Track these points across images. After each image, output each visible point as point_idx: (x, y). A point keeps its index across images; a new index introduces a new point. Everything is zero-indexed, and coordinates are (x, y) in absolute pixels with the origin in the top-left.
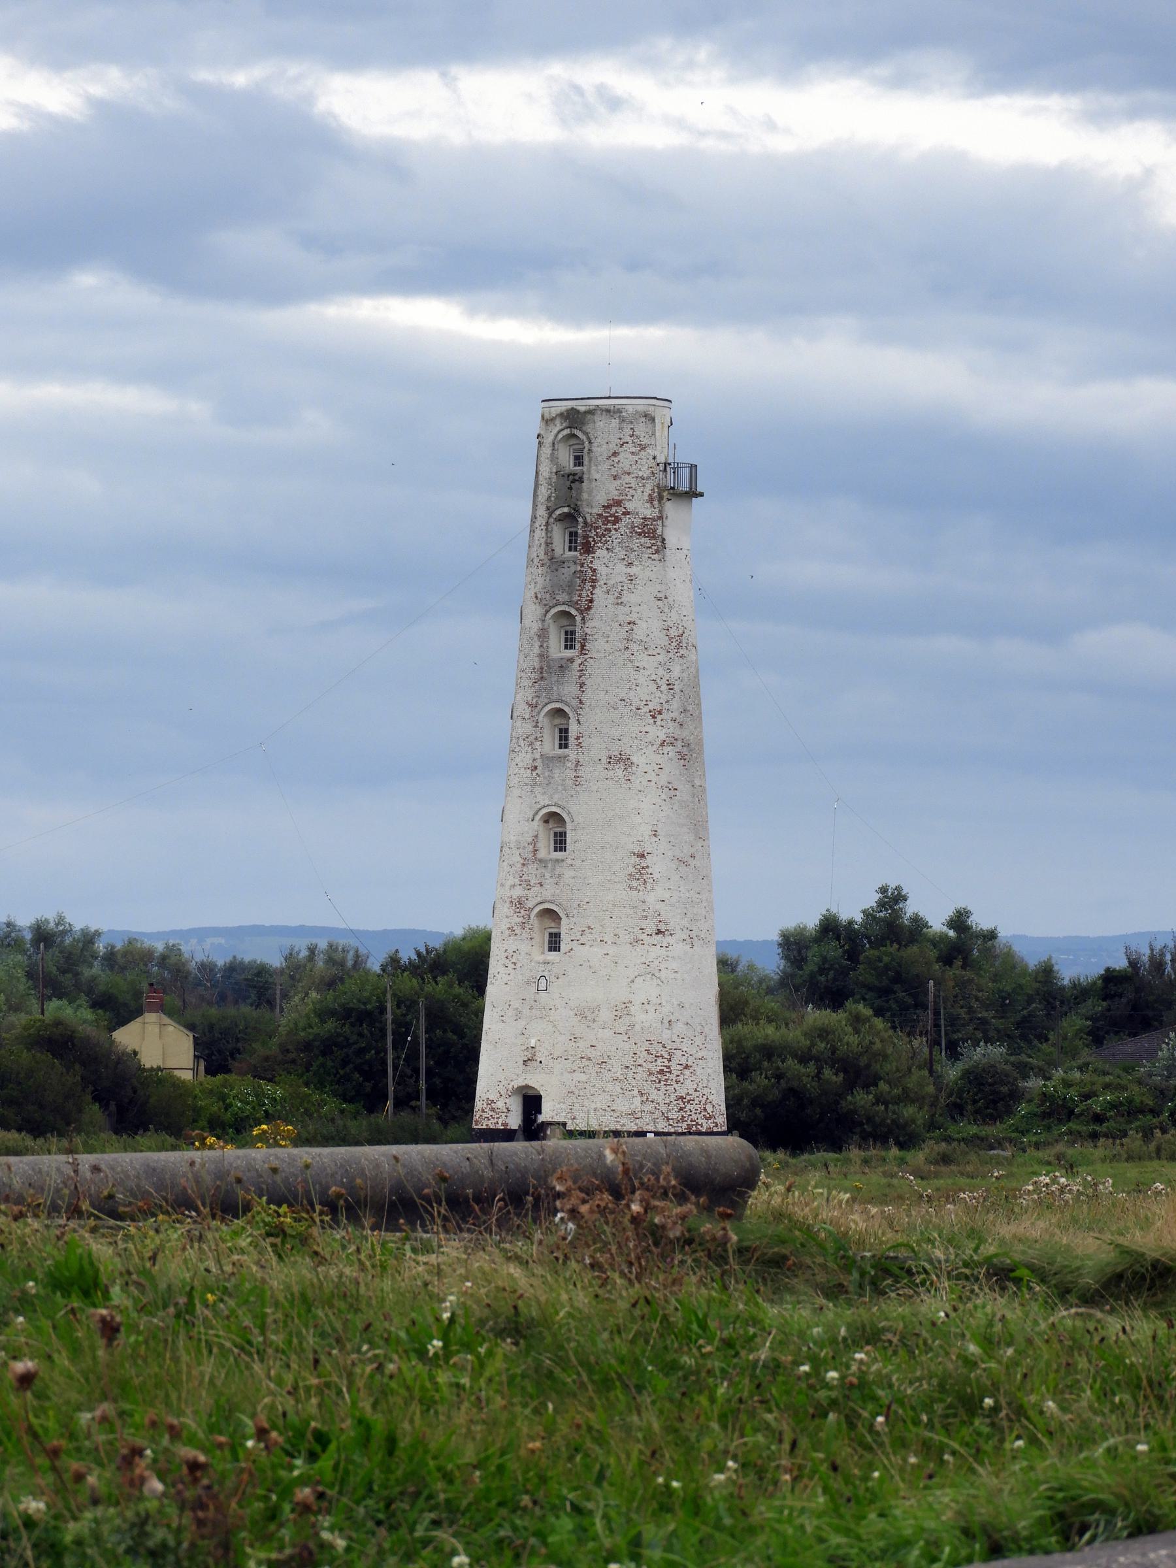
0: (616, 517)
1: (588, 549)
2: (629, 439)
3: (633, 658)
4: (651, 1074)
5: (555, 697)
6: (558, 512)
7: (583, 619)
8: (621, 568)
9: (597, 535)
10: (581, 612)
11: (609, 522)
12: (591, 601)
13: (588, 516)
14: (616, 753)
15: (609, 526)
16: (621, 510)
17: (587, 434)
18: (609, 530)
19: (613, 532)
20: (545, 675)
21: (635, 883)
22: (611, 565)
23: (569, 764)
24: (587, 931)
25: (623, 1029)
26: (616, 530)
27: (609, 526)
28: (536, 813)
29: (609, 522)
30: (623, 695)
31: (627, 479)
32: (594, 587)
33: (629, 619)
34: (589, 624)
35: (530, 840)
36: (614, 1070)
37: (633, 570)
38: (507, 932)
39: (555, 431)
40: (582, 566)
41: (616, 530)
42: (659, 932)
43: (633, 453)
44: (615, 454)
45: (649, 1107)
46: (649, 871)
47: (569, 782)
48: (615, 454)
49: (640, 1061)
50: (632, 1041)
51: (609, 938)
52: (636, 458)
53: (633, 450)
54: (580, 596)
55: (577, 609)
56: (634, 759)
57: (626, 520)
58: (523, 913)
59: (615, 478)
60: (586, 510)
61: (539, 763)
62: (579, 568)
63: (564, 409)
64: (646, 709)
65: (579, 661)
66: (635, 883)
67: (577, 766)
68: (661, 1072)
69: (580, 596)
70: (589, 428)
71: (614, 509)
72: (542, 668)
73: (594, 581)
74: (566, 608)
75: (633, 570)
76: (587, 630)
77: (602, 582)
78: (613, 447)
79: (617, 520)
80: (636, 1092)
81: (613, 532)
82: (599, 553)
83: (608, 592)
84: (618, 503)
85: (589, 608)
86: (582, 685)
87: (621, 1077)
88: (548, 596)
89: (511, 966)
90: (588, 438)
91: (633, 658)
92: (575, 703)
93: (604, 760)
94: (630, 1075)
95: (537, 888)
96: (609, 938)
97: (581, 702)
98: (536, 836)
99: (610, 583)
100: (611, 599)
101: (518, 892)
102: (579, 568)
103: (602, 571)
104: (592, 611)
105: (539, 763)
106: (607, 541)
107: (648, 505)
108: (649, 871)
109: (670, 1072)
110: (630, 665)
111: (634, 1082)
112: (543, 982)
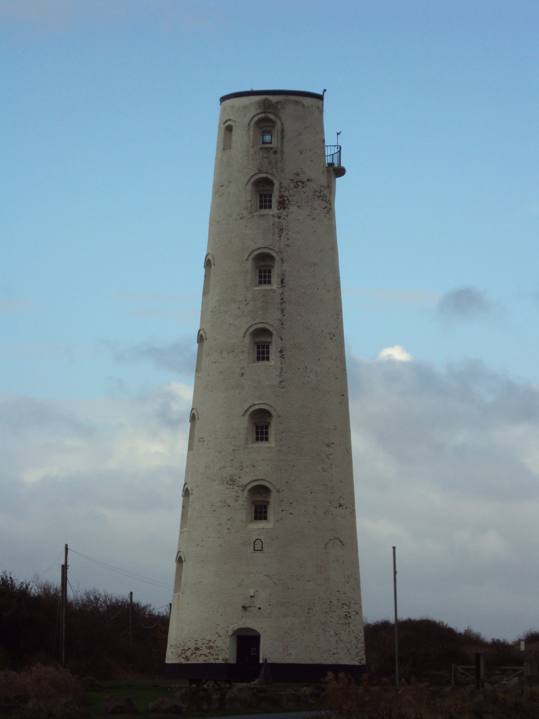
17: (279, 118)
86: (283, 310)
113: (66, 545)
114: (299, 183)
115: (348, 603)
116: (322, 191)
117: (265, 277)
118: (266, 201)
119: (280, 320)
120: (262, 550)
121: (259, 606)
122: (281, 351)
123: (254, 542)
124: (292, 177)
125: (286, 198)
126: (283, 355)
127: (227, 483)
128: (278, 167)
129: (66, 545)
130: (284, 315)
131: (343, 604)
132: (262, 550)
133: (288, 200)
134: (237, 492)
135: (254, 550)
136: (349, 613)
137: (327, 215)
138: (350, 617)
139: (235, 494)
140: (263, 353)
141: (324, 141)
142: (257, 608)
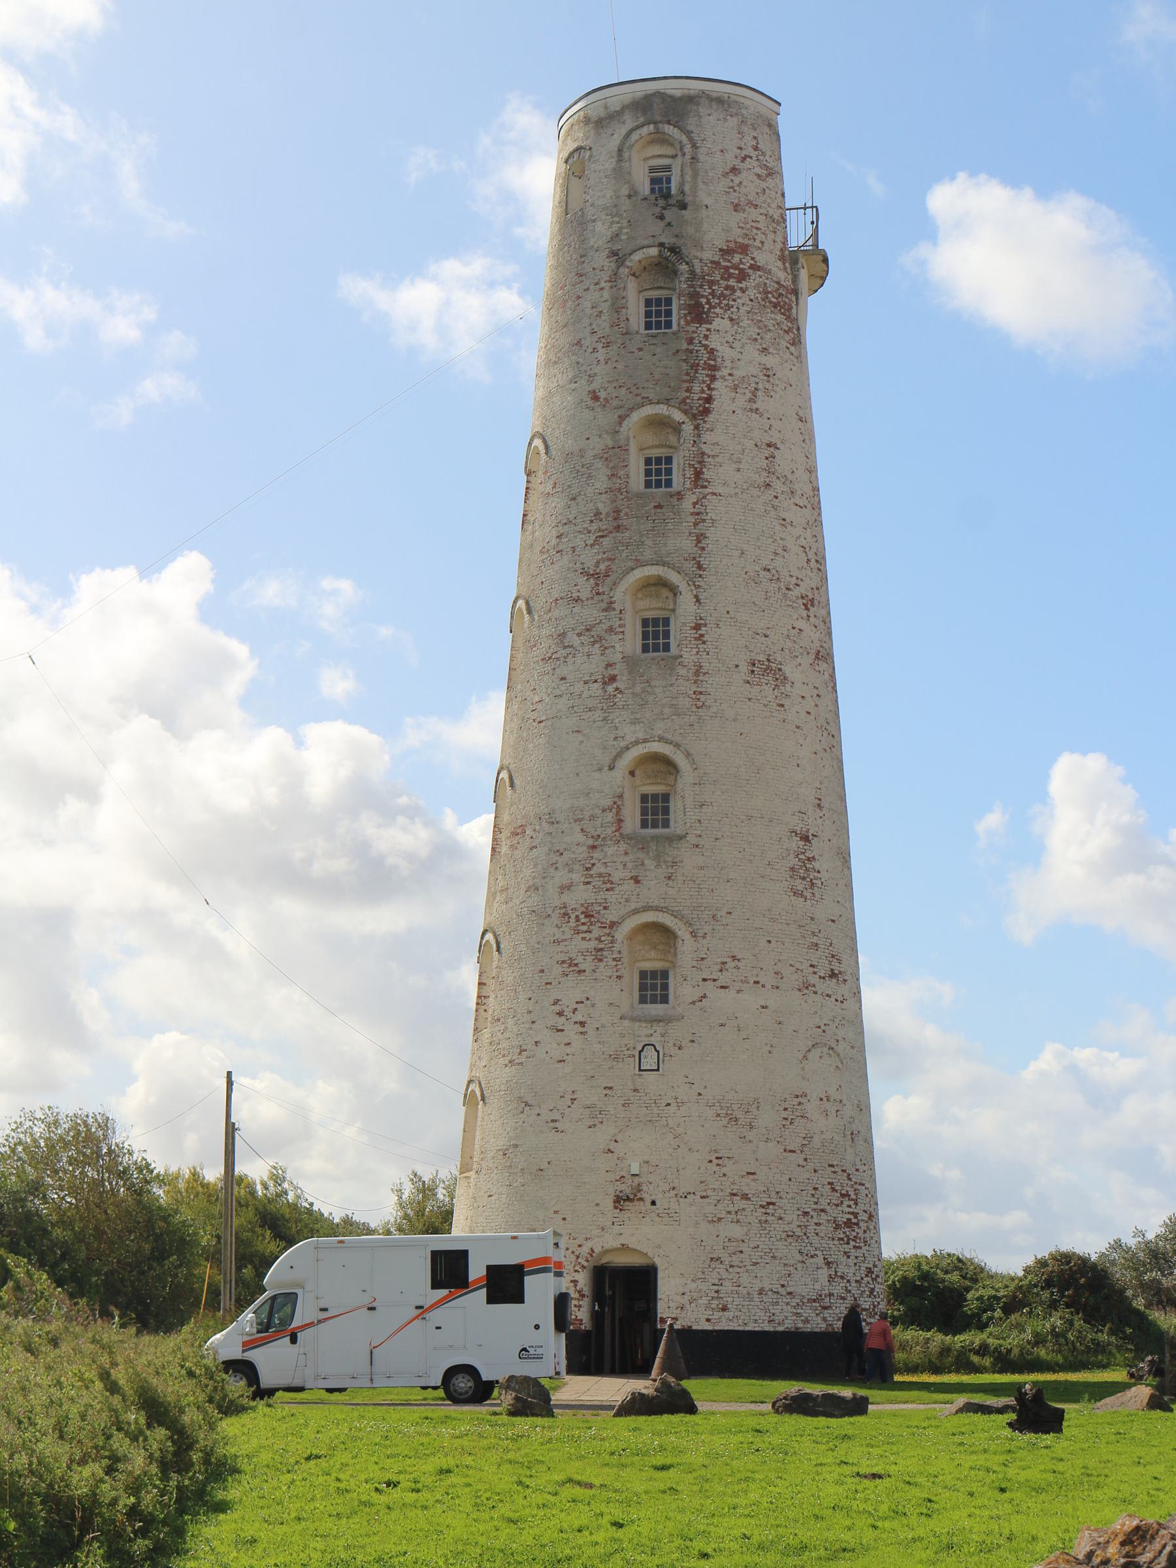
0: (742, 271)
1: (698, 314)
2: (753, 154)
3: (776, 502)
4: (837, 1227)
5: (648, 554)
6: (637, 257)
7: (697, 427)
8: (751, 352)
9: (713, 294)
10: (694, 417)
11: (731, 276)
12: (709, 400)
13: (696, 262)
14: (762, 657)
15: (732, 282)
16: (748, 262)
17: (688, 134)
18: (733, 290)
19: (738, 293)
20: (624, 522)
21: (800, 885)
22: (737, 344)
23: (683, 672)
24: (731, 964)
25: (795, 1144)
26: (743, 291)
27: (732, 282)
28: (619, 755)
29: (731, 276)
30: (765, 562)
31: (754, 214)
32: (713, 378)
33: (767, 439)
34: (706, 437)
35: (608, 802)
36: (788, 1218)
37: (769, 361)
38: (557, 970)
39: (624, 131)
40: (690, 341)
41: (743, 291)
42: (833, 975)
43: (758, 176)
44: (734, 170)
45: (838, 1288)
46: (817, 865)
47: (685, 702)
48: (734, 170)
49: (823, 1203)
50: (810, 1166)
51: (768, 979)
52: (764, 185)
53: (758, 170)
54: (688, 390)
55: (685, 412)
56: (787, 670)
57: (755, 279)
58: (596, 932)
59: (737, 208)
60: (691, 252)
61: (619, 670)
62: (685, 346)
63: (639, 95)
64: (797, 592)
65: (694, 498)
66: (800, 885)
67: (697, 673)
68: (848, 1223)
69: (688, 390)
70: (691, 123)
71: (737, 258)
72: (617, 512)
73: (714, 368)
74: (662, 409)
75: (769, 361)
76: (706, 449)
77: (725, 372)
78: (730, 159)
79: (742, 276)
80: (820, 1260)
81: (738, 293)
82: (717, 323)
83: (735, 388)
84: (744, 249)
85: (706, 412)
86: (700, 538)
87: (798, 1232)
88: (623, 391)
89: (571, 1031)
90: (691, 139)
91: (776, 502)
92: (690, 566)
93: (744, 668)
94: (812, 1228)
95: (629, 886)
96: (768, 979)
97: (700, 567)
98: (621, 796)
99: (738, 374)
100: (741, 401)
101: (580, 896)
102: (685, 346)
103: (724, 351)
104: (711, 418)
105: (619, 670)
106: (729, 307)
107: (779, 264)
108: (817, 865)
109: (857, 1224)
110: (773, 513)
111: (815, 1241)
112: (649, 1060)
113: (229, 1074)
114: (732, 271)
115: (852, 1193)
116: (780, 295)
117: (659, 472)
118: (658, 314)
119: (694, 559)
120: (658, 1070)
121: (653, 1198)
122: (697, 627)
123: (640, 1052)
124: (716, 259)
125: (704, 301)
126: (702, 636)
127: (577, 919)
128: (682, 263)
129: (229, 1074)
130: (703, 549)
131: (843, 1195)
132: (658, 1070)
133: (708, 302)
134: (599, 939)
135: (640, 1070)
136: (855, 1215)
137: (792, 349)
138: (857, 1224)
139: (593, 944)
140: (656, 635)
141: (783, 195)
142: (648, 1203)
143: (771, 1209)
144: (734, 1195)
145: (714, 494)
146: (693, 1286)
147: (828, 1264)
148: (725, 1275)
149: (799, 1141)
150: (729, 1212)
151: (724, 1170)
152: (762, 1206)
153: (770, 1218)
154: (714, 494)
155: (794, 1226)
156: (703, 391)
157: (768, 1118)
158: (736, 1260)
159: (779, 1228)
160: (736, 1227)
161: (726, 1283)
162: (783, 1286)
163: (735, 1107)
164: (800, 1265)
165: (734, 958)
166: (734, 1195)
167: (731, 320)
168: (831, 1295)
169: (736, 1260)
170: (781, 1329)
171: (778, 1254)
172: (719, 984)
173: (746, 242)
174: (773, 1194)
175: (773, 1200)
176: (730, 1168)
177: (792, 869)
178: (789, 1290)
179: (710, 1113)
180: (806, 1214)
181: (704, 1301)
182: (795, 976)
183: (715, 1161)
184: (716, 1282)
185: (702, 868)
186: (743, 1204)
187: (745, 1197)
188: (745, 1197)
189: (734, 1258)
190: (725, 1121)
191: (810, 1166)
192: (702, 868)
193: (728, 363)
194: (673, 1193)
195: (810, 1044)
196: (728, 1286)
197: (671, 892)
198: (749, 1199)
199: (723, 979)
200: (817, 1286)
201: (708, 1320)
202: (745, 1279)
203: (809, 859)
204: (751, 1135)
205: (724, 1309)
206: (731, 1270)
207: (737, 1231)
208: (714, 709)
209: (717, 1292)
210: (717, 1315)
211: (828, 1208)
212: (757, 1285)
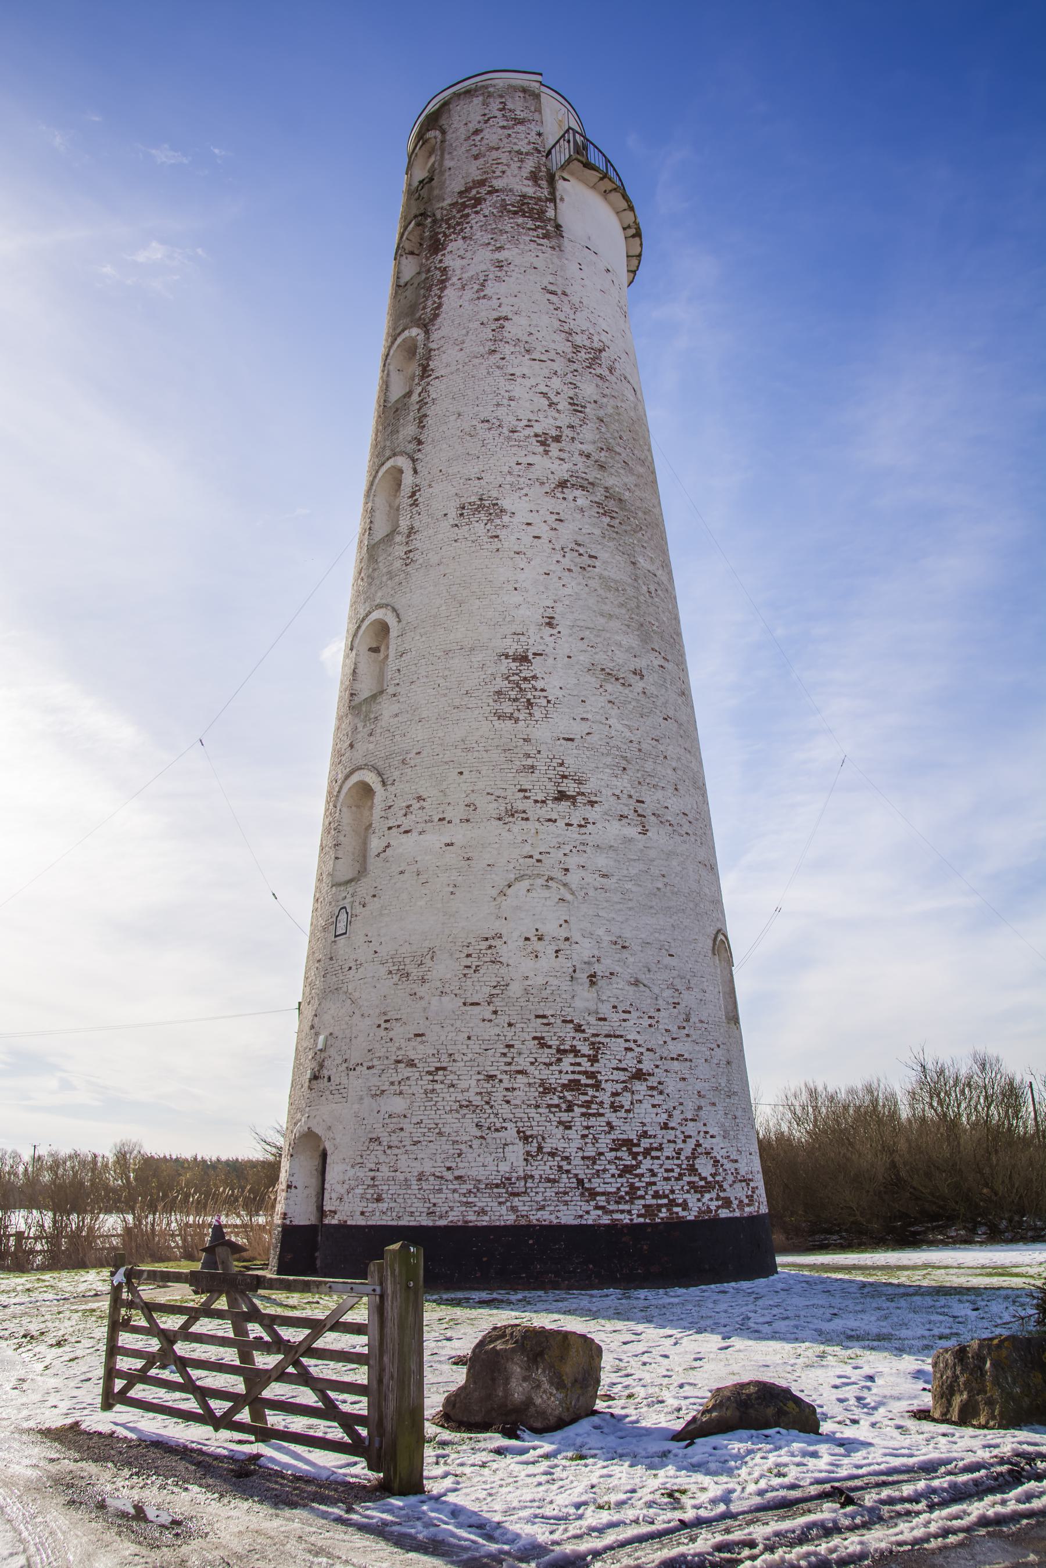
12: (440, 306)
14: (473, 499)
19: (473, 216)
21: (507, 708)
24: (416, 805)
32: (442, 290)
43: (503, 127)
44: (477, 132)
45: (544, 1167)
48: (477, 132)
49: (523, 1063)
50: (503, 1020)
56: (505, 504)
59: (476, 157)
68: (574, 1085)
71: (474, 192)
75: (501, 256)
76: (432, 346)
79: (478, 201)
80: (511, 1133)
84: (482, 183)
87: (477, 1100)
93: (453, 513)
94: (498, 1096)
96: (455, 813)
104: (439, 320)
106: (462, 230)
108: (539, 684)
110: (498, 372)
111: (505, 1111)
143: (439, 1076)
144: (399, 1062)
145: (437, 378)
146: (351, 1173)
147: (526, 1139)
148: (382, 1158)
149: (487, 990)
150: (392, 1083)
151: (391, 1034)
152: (429, 1073)
153: (438, 1086)
154: (437, 378)
155: (471, 1095)
156: (435, 302)
157: (444, 969)
158: (394, 1139)
159: (450, 1097)
160: (398, 1099)
161: (384, 1168)
162: (449, 1169)
163: (407, 961)
164: (476, 1143)
165: (420, 798)
166: (399, 1062)
167: (464, 238)
168: (527, 1177)
169: (394, 1139)
170: (442, 1223)
171: (446, 1130)
172: (402, 829)
173: (484, 177)
174: (444, 1058)
175: (444, 1065)
176: (398, 1031)
177: (499, 693)
178: (457, 1173)
179: (383, 971)
180: (491, 1077)
181: (359, 1191)
182: (495, 805)
183: (384, 1025)
184: (373, 1166)
185: (397, 715)
186: (407, 1072)
187: (411, 1064)
188: (411, 1064)
189: (394, 1137)
190: (396, 978)
191: (503, 1020)
192: (397, 715)
193: (458, 272)
194: (345, 1065)
195: (512, 876)
196: (385, 1172)
197: (371, 746)
198: (415, 1066)
199: (407, 823)
200: (504, 1167)
201: (362, 1213)
202: (403, 1162)
203: (525, 679)
204: (422, 991)
205: (379, 1200)
206: (389, 1152)
207: (398, 1105)
208: (421, 561)
209: (373, 1179)
210: (372, 1206)
211: (531, 1069)
212: (417, 1168)
